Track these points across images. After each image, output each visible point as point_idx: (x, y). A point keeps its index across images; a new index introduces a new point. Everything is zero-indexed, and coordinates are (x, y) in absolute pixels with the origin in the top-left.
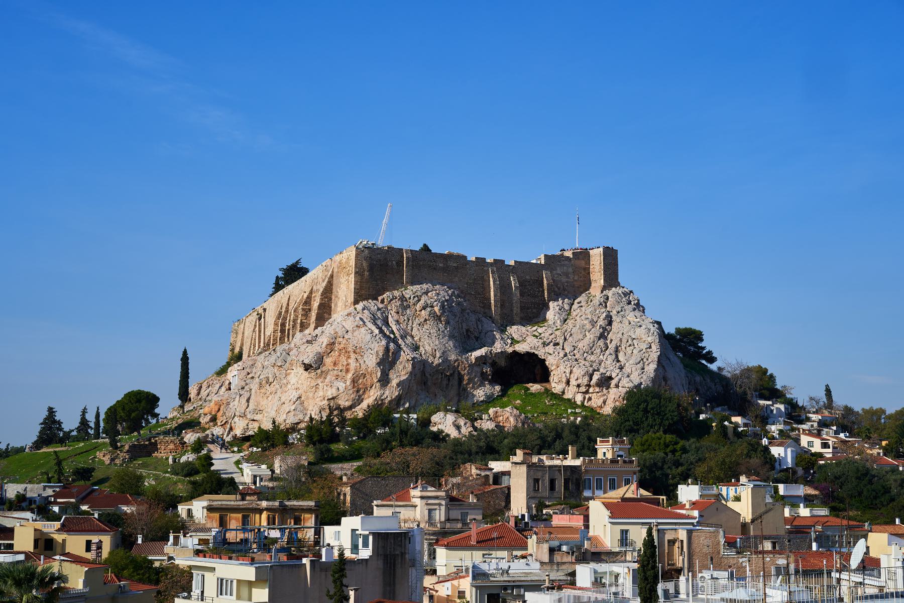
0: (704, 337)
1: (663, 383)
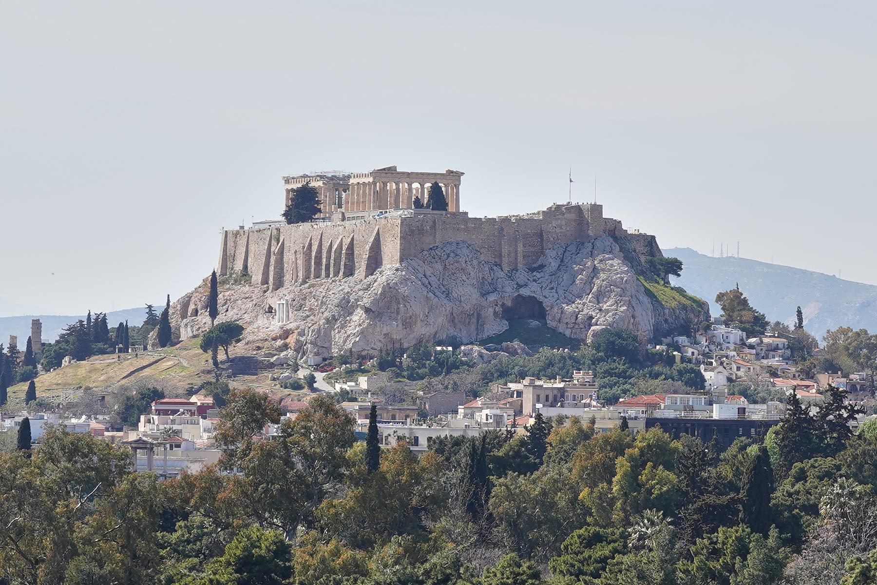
0: (683, 266)
1: (632, 320)
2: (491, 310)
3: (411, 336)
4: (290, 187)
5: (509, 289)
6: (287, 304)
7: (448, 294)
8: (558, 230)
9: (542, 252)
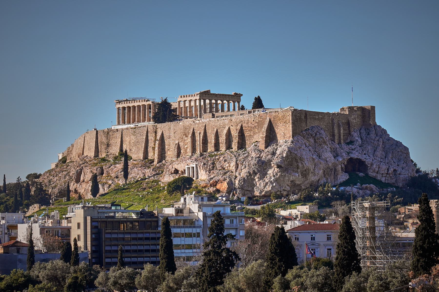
2: (340, 166)
3: (306, 182)
4: (121, 106)
5: (344, 154)
6: (197, 167)
7: (320, 157)
8: (355, 121)
9: (350, 134)
